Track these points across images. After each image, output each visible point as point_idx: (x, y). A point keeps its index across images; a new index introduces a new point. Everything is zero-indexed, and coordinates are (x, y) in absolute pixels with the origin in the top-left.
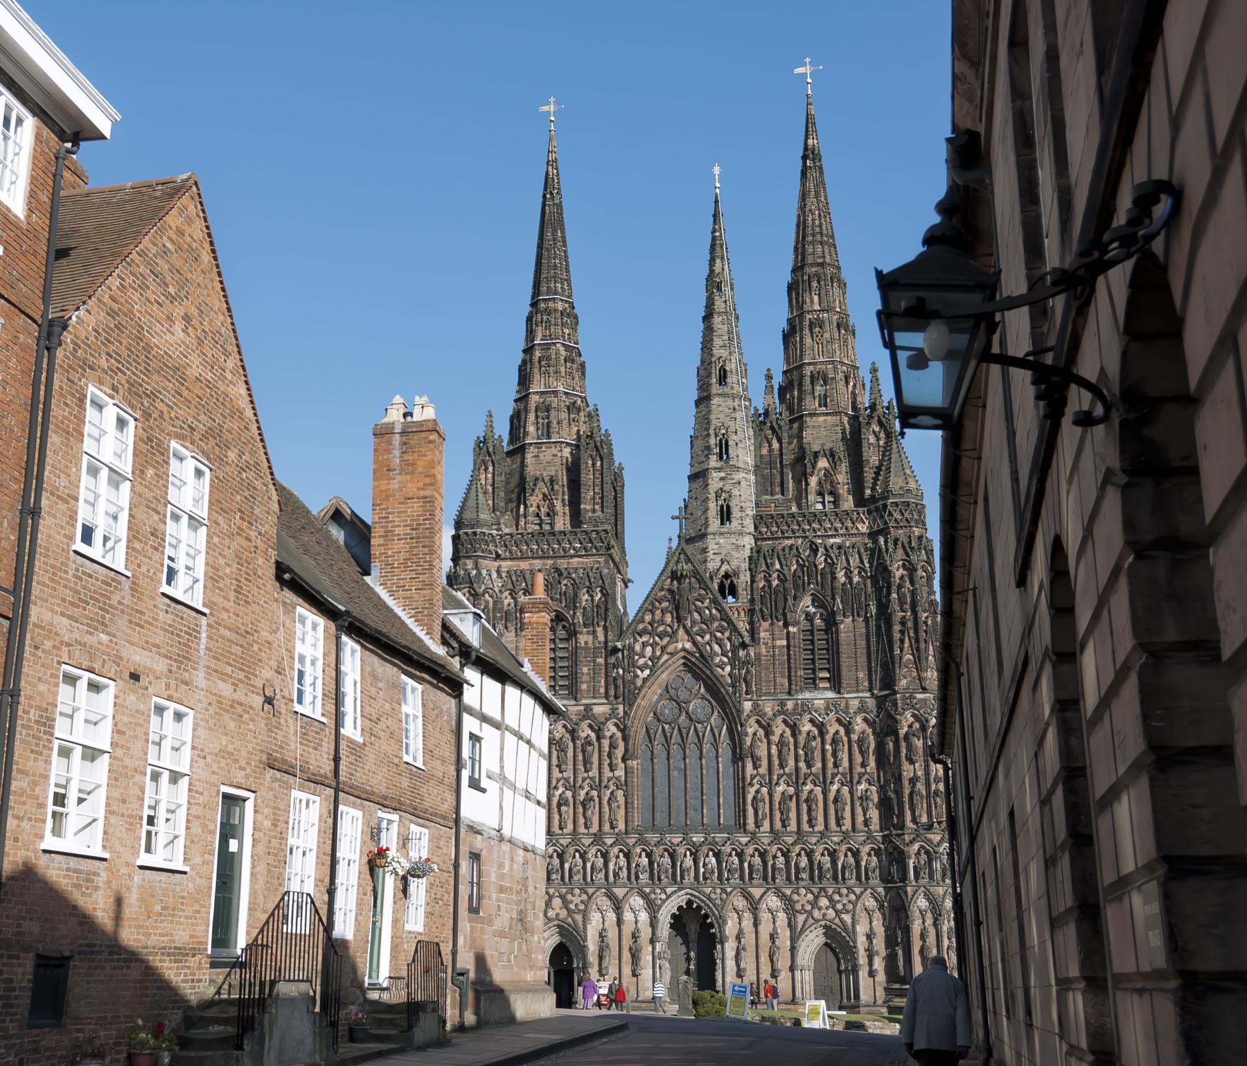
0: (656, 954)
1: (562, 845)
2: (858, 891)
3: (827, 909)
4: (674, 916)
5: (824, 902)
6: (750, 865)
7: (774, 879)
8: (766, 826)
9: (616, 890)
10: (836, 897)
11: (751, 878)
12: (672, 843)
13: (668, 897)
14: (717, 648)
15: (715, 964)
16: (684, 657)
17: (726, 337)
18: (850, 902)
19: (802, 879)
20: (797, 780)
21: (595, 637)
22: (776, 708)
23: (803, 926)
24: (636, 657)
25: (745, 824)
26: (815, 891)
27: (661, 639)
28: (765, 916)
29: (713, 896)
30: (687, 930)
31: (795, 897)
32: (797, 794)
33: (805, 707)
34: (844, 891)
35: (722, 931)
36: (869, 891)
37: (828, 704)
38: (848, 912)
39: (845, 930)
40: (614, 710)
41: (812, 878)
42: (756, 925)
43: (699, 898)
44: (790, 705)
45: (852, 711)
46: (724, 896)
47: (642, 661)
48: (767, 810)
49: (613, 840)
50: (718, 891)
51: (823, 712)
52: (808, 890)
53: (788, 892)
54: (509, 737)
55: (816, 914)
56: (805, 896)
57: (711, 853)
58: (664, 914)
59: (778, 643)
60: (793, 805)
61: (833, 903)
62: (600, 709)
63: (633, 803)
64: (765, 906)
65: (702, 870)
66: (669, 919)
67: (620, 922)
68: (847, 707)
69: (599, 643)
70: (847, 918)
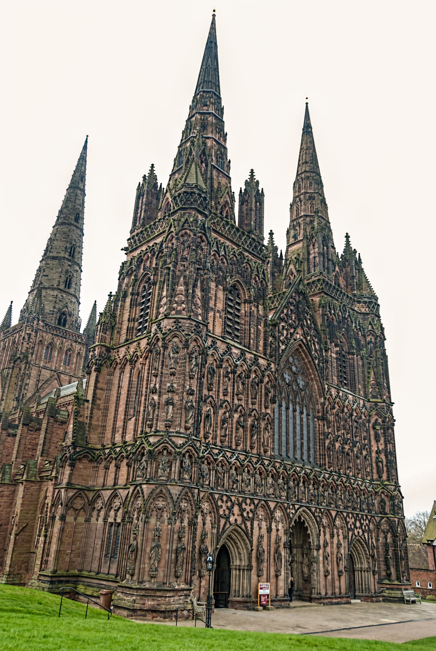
5: (358, 524)
9: (270, 503)
10: (362, 522)
13: (296, 512)
16: (300, 345)
17: (81, 202)
18: (367, 524)
21: (258, 311)
23: (351, 539)
34: (365, 517)
40: (269, 365)
42: (332, 536)
44: (341, 394)
46: (320, 515)
61: (361, 524)
62: (262, 361)
67: (269, 530)
70: (366, 535)
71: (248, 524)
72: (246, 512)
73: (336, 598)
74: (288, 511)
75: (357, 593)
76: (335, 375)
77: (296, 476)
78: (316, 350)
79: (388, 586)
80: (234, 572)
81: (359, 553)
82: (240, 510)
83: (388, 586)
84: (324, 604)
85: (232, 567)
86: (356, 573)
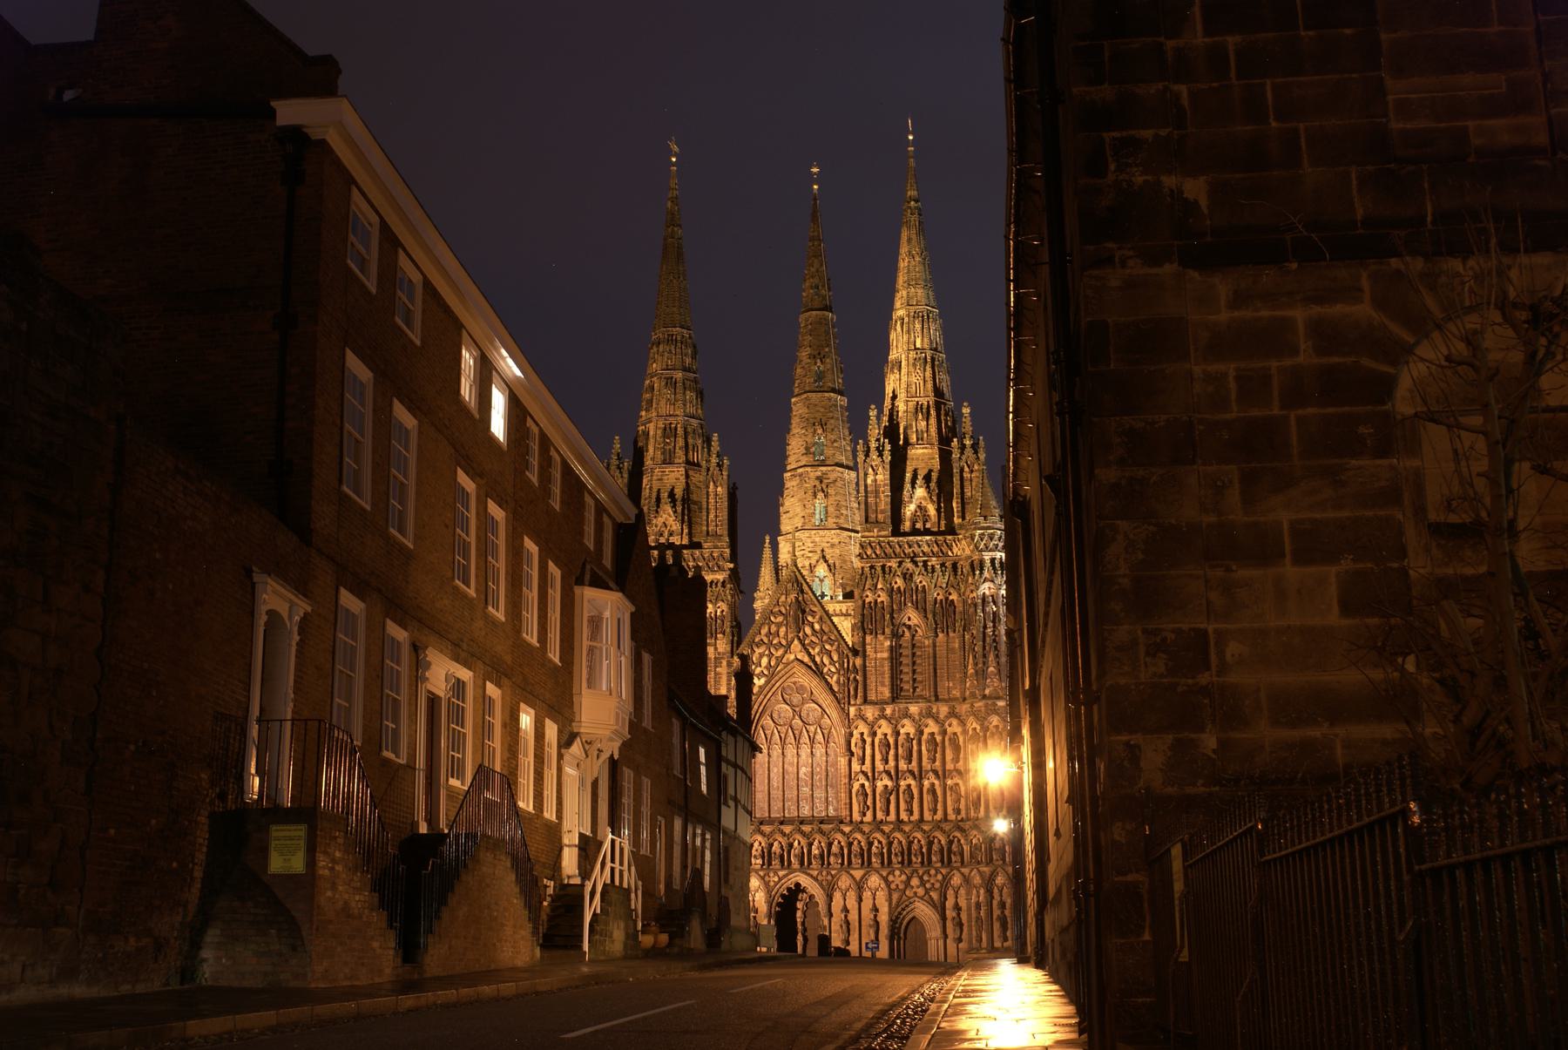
2: (944, 871)
3: (918, 887)
5: (915, 882)
8: (869, 814)
10: (926, 878)
13: (780, 879)
14: (826, 660)
18: (938, 881)
20: (896, 776)
21: (716, 649)
22: (877, 713)
23: (898, 902)
24: (753, 667)
27: (777, 650)
28: (867, 895)
32: (898, 786)
33: (907, 715)
34: (933, 872)
36: (955, 871)
37: (921, 711)
42: (860, 900)
44: (888, 711)
45: (942, 716)
47: (758, 670)
50: (824, 873)
51: (917, 717)
53: (884, 874)
54: (739, 772)
56: (900, 876)
59: (879, 655)
60: (893, 798)
61: (923, 883)
68: (938, 713)
69: (719, 654)
70: (934, 895)
74: (767, 878)
76: (883, 685)
78: (832, 662)
79: (975, 956)
83: (975, 956)
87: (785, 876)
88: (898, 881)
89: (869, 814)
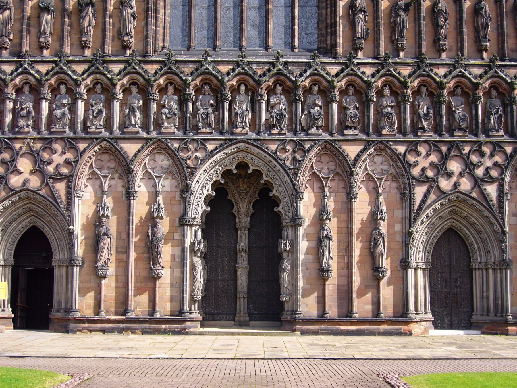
0: (187, 244)
1: (38, 72)
4: (216, 186)
5: (455, 166)
6: (343, 109)
7: (378, 131)
10: (474, 158)
11: (343, 127)
12: (219, 72)
15: (280, 258)
19: (423, 128)
23: (423, 201)
25: (335, 45)
26: (444, 149)
29: (282, 155)
30: (235, 210)
31: (411, 158)
35: (296, 209)
38: (491, 180)
39: (489, 208)
41: (437, 129)
43: (258, 156)
48: (370, 25)
49: (121, 66)
52: (434, 146)
53: (401, 149)
55: (445, 184)
56: (428, 155)
57: (279, 89)
58: (202, 181)
63: (156, 11)
64: (362, 170)
65: (264, 116)
66: (208, 191)
70: (492, 190)
71: (61, 187)
72: (53, 165)
73: (352, 324)
75: (476, 317)
77: (215, 81)
80: (59, 273)
81: (478, 232)
82: (35, 163)
84: (304, 333)
85: (54, 263)
86: (477, 275)
87: (216, 149)
88: (424, 163)
89: (368, 46)
